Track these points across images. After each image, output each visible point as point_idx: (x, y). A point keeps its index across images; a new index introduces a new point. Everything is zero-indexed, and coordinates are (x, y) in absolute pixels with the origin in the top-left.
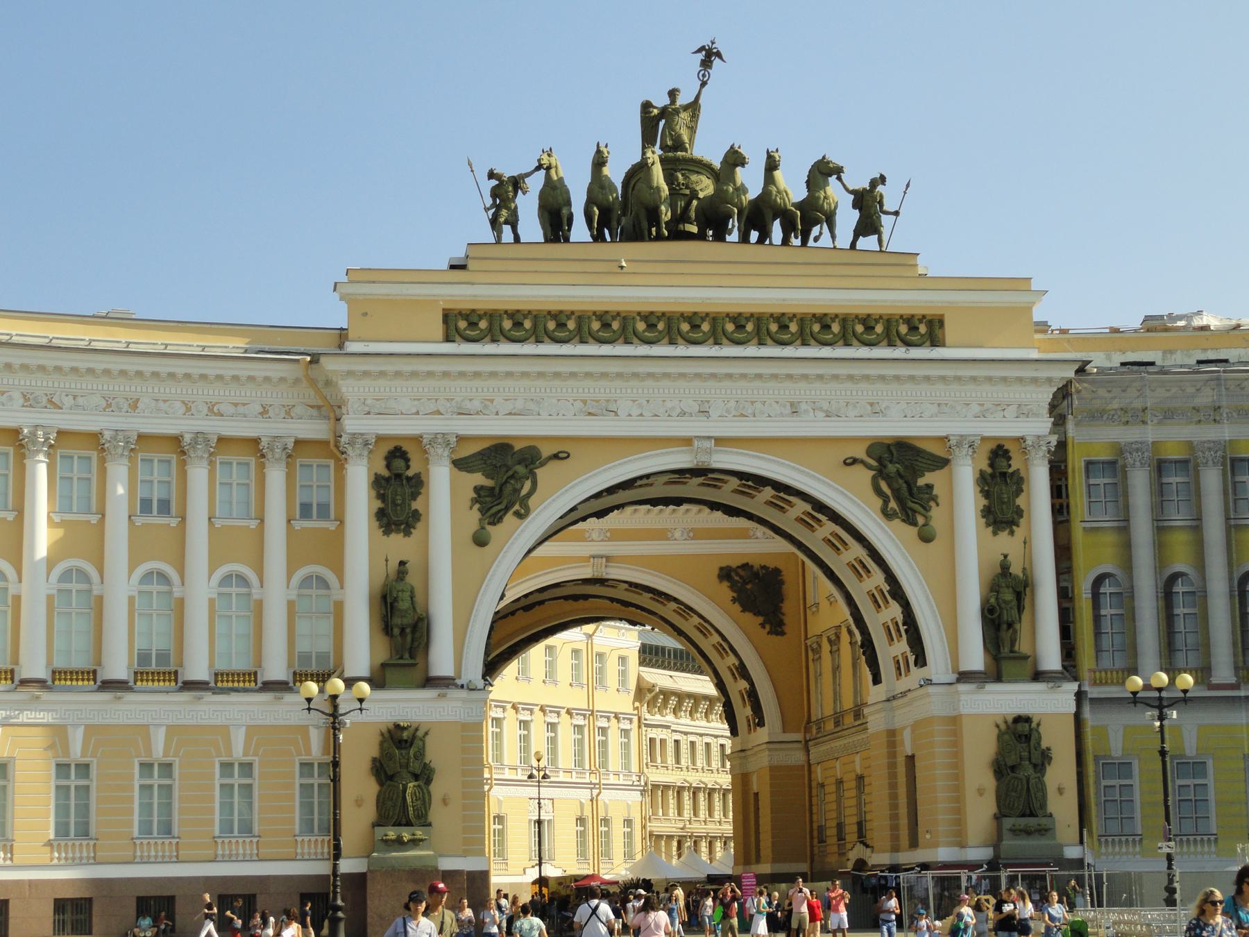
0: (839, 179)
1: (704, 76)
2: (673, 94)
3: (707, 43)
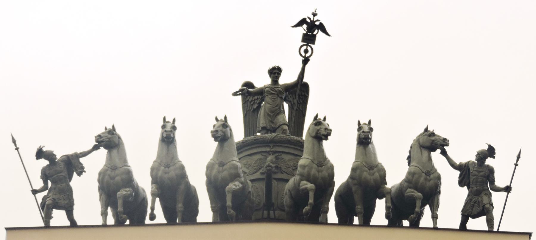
0: (444, 153)
1: (306, 51)
2: (275, 72)
3: (307, 14)
